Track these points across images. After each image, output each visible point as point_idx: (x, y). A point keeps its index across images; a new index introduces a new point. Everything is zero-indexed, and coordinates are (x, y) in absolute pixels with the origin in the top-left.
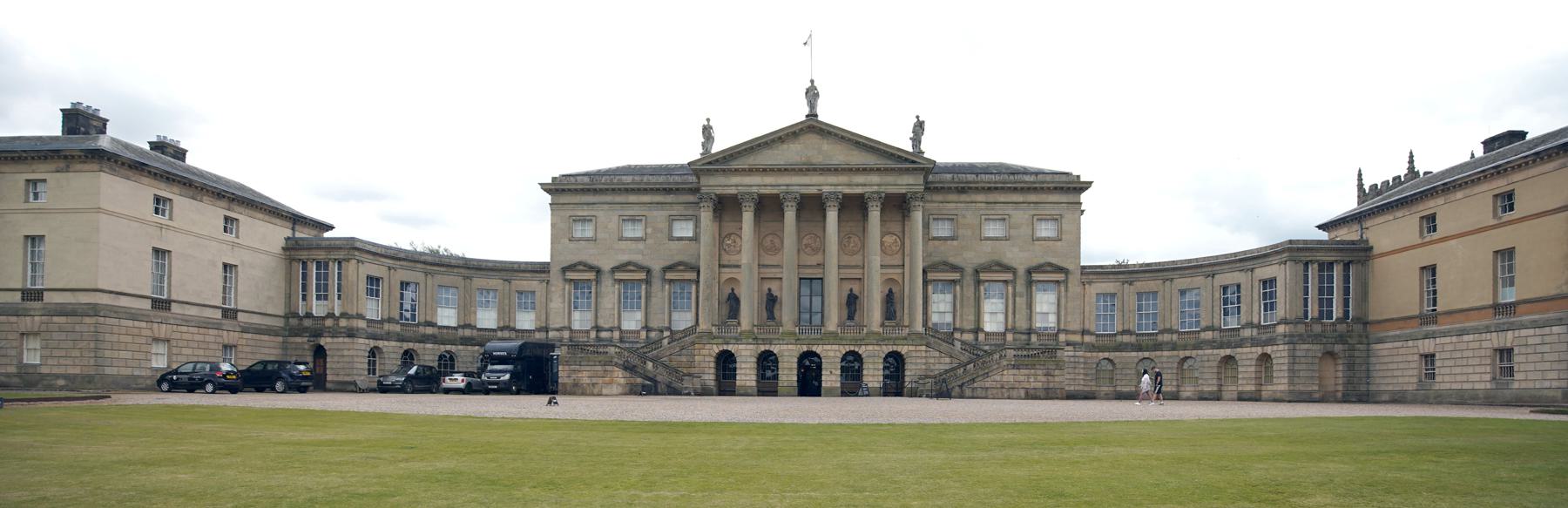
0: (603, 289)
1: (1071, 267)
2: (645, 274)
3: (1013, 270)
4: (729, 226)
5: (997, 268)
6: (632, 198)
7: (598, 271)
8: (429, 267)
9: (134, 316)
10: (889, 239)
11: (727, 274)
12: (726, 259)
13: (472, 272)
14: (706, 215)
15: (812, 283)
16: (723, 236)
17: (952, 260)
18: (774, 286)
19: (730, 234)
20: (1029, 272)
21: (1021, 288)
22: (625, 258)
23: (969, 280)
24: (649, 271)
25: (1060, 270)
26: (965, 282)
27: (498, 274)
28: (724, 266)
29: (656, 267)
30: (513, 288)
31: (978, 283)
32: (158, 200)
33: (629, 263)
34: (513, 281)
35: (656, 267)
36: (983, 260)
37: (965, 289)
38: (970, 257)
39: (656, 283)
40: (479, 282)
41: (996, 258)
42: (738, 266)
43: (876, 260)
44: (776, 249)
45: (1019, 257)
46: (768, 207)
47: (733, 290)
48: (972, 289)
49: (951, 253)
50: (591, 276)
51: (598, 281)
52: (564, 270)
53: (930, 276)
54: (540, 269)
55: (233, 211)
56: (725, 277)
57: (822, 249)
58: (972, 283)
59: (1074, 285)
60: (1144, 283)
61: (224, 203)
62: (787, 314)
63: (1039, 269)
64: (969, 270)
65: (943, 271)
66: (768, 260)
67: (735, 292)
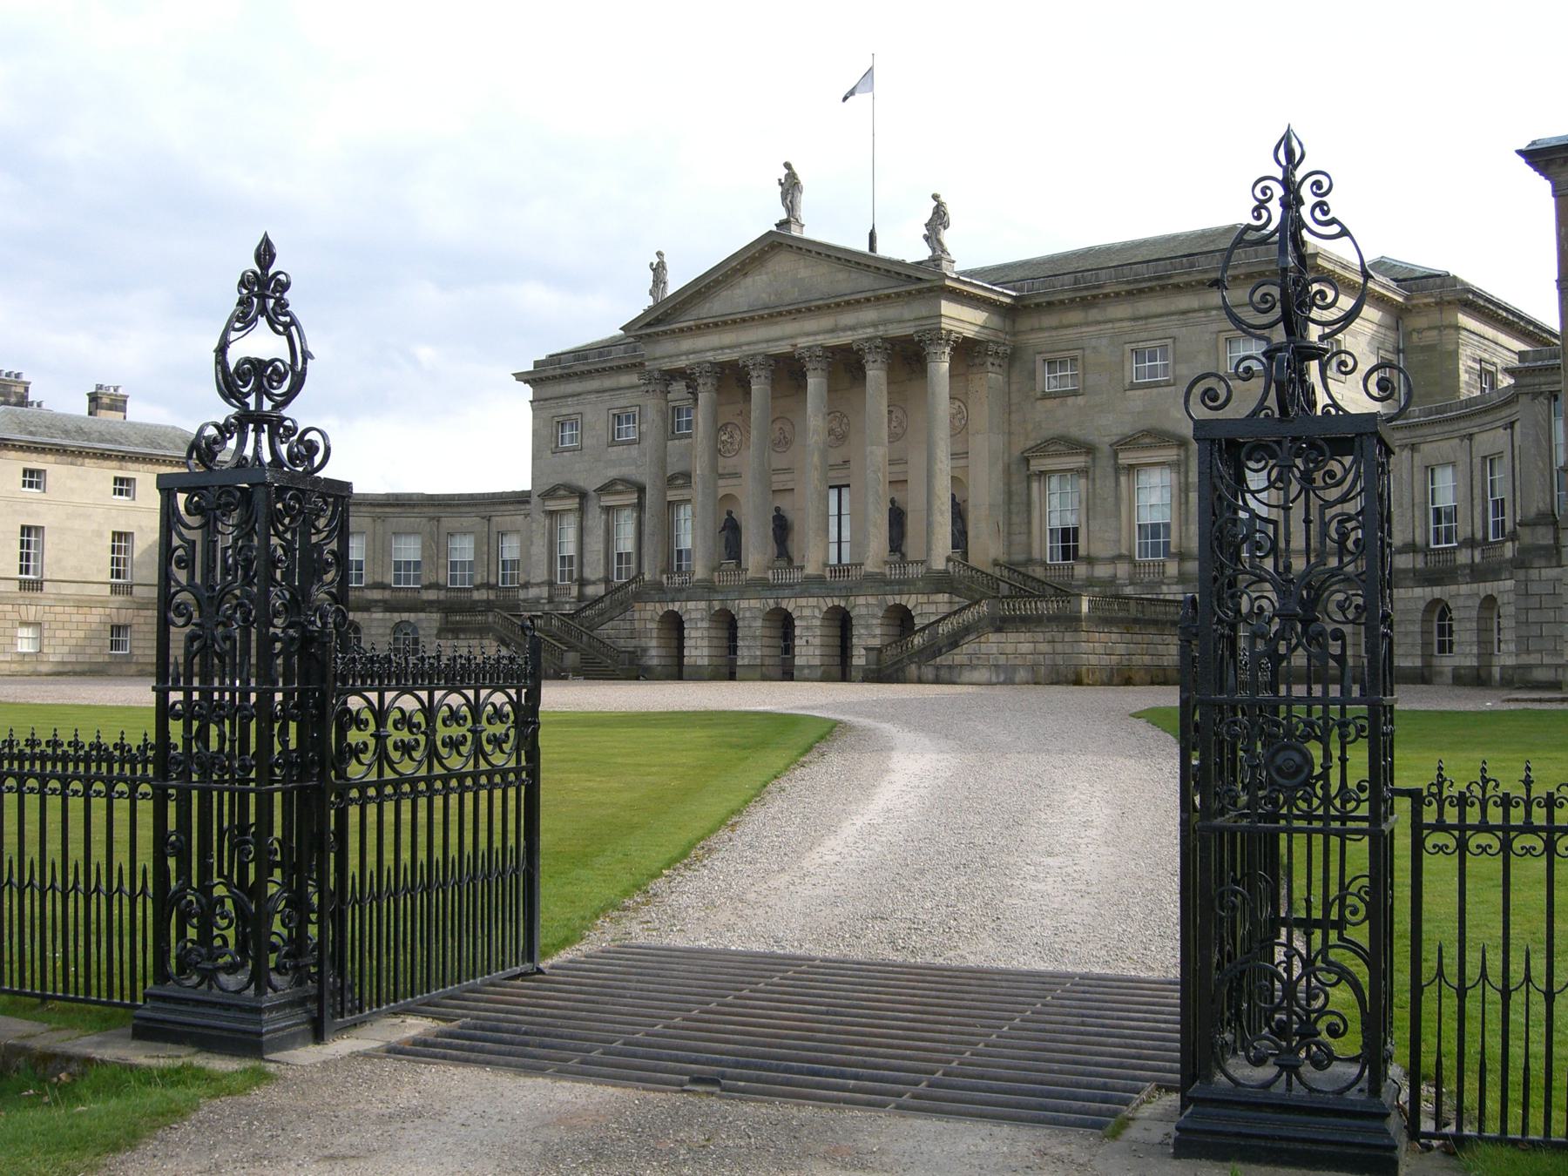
0: (590, 522)
2: (636, 496)
5: (1147, 440)
7: (583, 495)
8: (378, 510)
13: (441, 509)
16: (720, 425)
17: (1075, 432)
18: (784, 503)
19: (726, 425)
22: (613, 473)
23: (1104, 462)
26: (1098, 472)
27: (474, 509)
28: (721, 476)
30: (494, 529)
31: (1117, 469)
32: (28, 472)
33: (613, 482)
34: (494, 519)
36: (1127, 430)
37: (1098, 482)
40: (448, 523)
41: (1151, 422)
42: (736, 475)
46: (732, 377)
47: (729, 513)
48: (1110, 482)
49: (1066, 419)
51: (582, 511)
53: (1036, 465)
54: (520, 499)
55: (127, 469)
56: (721, 492)
58: (1110, 470)
60: (1434, 445)
61: (115, 464)
62: (756, 554)
64: (1105, 449)
65: (1058, 455)
66: (778, 461)
67: (734, 515)
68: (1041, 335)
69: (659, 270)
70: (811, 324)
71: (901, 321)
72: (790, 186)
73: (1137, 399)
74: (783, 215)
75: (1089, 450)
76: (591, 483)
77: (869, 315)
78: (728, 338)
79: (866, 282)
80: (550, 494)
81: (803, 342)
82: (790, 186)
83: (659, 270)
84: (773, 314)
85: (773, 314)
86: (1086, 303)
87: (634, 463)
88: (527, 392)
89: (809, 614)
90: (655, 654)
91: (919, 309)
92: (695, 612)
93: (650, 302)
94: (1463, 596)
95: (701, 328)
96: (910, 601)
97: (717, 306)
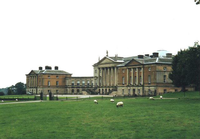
40: (87, 80)
46: (103, 68)
50: (96, 78)
51: (97, 79)
69: (99, 58)
70: (108, 65)
72: (107, 52)
74: (107, 55)
77: (111, 64)
80: (95, 77)
82: (107, 52)
83: (99, 58)
84: (106, 64)
85: (106, 64)
88: (93, 67)
92: (101, 89)
93: (99, 61)
97: (103, 62)
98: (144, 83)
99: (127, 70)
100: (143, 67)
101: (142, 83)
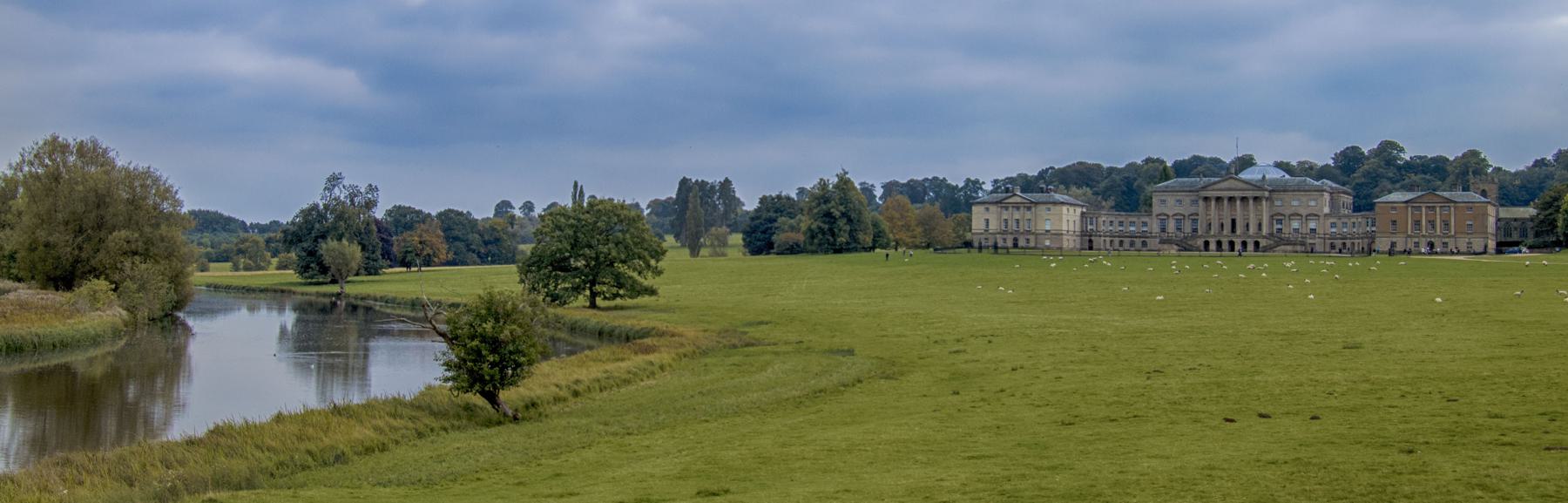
1: (1320, 214)
3: (1302, 216)
4: (1209, 204)
6: (1179, 194)
7: (1168, 216)
9: (1042, 234)
10: (1259, 207)
11: (1208, 217)
12: (1208, 213)
14: (1201, 203)
15: (1234, 222)
20: (1307, 216)
21: (1304, 219)
22: (1176, 212)
23: (1287, 218)
24: (1184, 216)
25: (1316, 215)
29: (1186, 214)
35: (1186, 214)
36: (1292, 212)
38: (1287, 212)
39: (1187, 220)
43: (1252, 215)
44: (1223, 210)
45: (1304, 212)
46: (1218, 199)
50: (1165, 217)
52: (1157, 215)
57: (1235, 210)
59: (1321, 219)
63: (1310, 215)
66: (1221, 213)
68: (1275, 195)
71: (1258, 194)
73: (1294, 208)
75: (1284, 216)
76: (1170, 214)
77: (1251, 192)
78: (1219, 192)
79: (1250, 187)
81: (1236, 195)
86: (1284, 191)
87: (1193, 210)
89: (1238, 242)
90: (1202, 248)
91: (1261, 192)
94: (1356, 241)
95: (1213, 190)
96: (1259, 240)
98: (1455, 233)
99: (1410, 209)
100: (1455, 208)
101: (1453, 233)
